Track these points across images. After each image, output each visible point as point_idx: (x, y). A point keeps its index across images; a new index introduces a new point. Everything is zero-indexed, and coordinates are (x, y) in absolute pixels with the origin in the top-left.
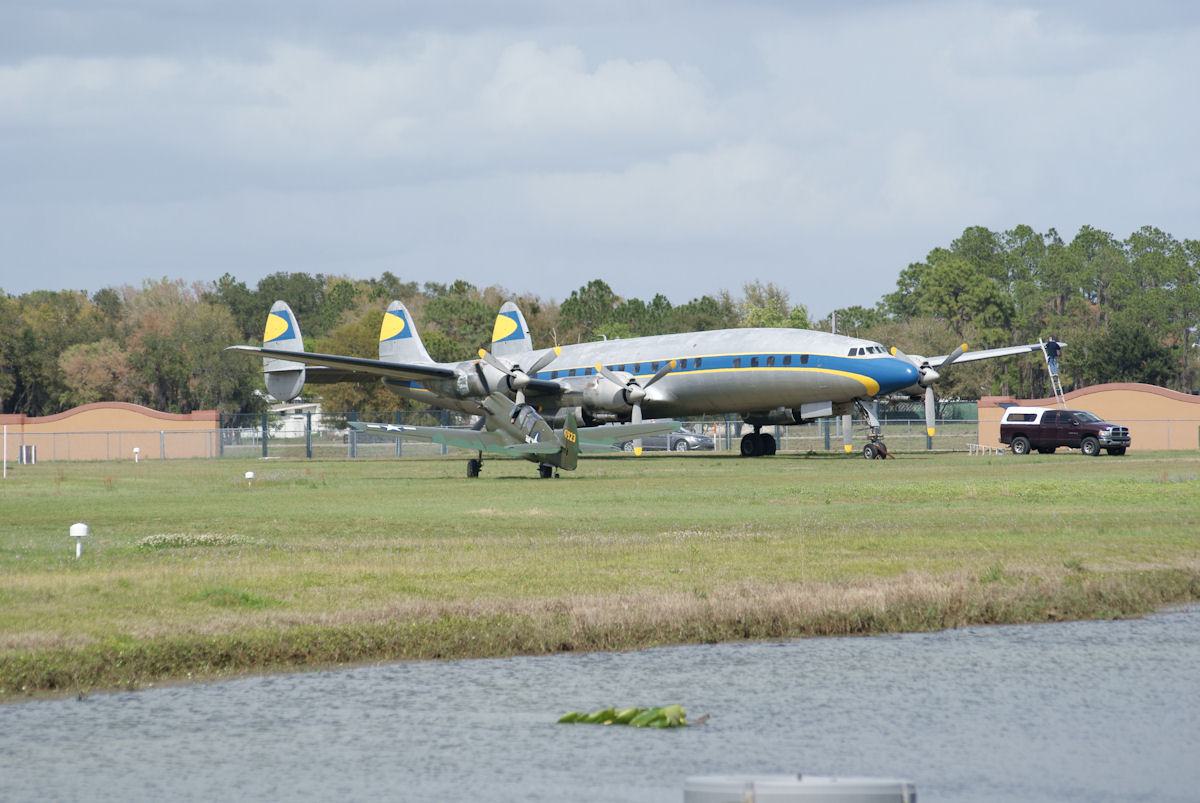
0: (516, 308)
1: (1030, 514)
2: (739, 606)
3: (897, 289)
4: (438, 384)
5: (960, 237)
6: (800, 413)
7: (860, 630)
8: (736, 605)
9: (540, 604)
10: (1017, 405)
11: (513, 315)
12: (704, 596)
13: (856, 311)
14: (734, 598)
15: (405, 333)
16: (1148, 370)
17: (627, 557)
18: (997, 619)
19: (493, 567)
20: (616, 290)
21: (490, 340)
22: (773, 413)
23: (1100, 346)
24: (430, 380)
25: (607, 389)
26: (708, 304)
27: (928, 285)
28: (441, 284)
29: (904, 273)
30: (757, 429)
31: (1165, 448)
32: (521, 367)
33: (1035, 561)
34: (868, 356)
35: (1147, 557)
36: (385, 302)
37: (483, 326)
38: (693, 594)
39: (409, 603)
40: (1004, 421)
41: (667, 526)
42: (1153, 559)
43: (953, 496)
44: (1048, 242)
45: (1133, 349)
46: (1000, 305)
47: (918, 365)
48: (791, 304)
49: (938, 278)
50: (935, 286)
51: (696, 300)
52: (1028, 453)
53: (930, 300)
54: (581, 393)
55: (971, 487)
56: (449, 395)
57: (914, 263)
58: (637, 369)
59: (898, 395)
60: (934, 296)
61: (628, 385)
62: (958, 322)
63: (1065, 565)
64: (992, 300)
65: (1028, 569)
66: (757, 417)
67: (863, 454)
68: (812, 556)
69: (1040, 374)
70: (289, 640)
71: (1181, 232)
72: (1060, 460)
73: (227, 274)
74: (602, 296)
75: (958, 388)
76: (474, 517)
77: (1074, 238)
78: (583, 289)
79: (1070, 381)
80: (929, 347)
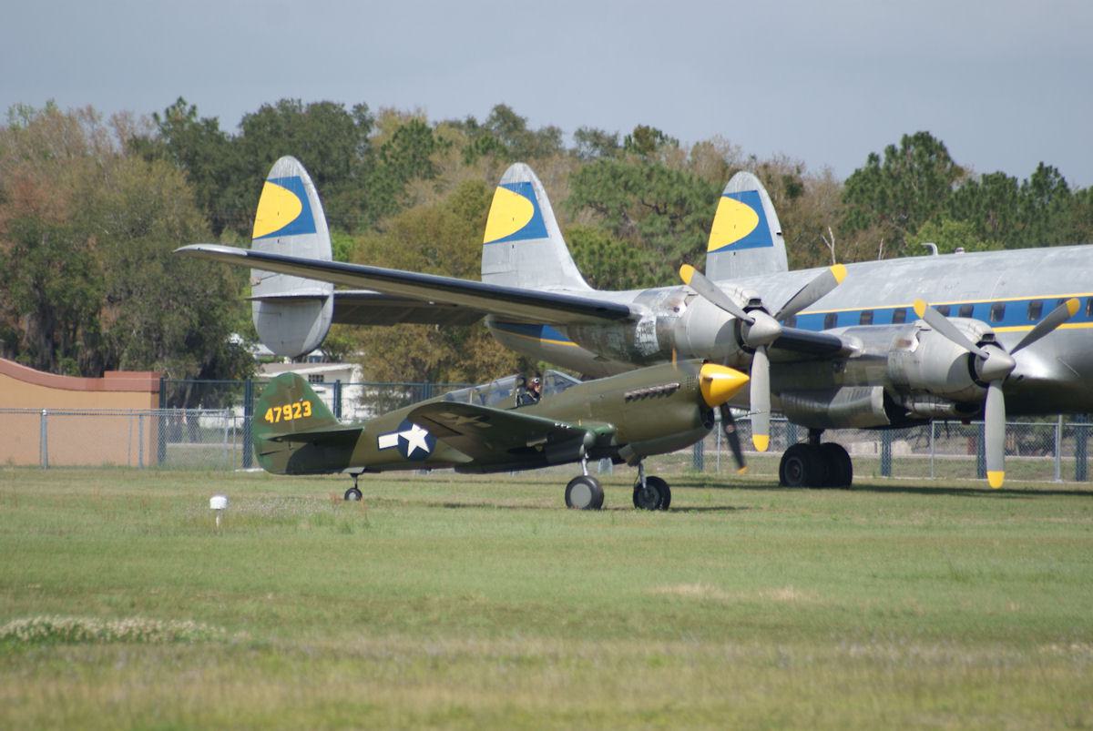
4: (596, 333)
24: (582, 324)
56: (619, 355)
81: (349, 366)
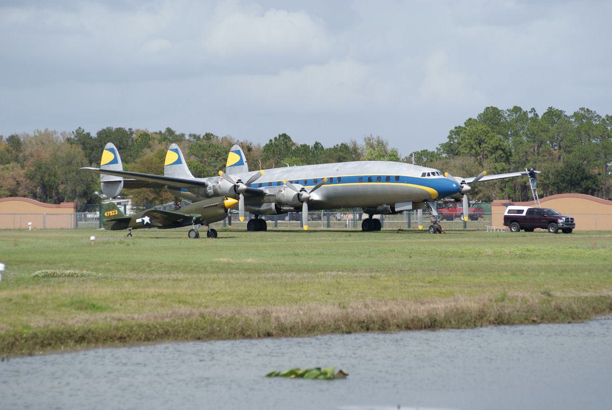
0: (239, 148)
1: (521, 265)
2: (363, 314)
3: (448, 140)
4: (196, 190)
5: (482, 112)
6: (394, 208)
7: (429, 327)
8: (362, 313)
9: (255, 310)
10: (512, 205)
11: (238, 152)
12: (344, 308)
13: (425, 153)
14: (361, 309)
15: (179, 162)
16: (584, 187)
17: (301, 286)
18: (505, 322)
19: (228, 290)
20: (294, 140)
21: (225, 166)
22: (380, 208)
23: (558, 174)
24: (192, 187)
25: (289, 193)
26: (344, 147)
27: (465, 138)
28: (198, 134)
29: (452, 132)
30: (371, 216)
31: (594, 229)
32: (242, 181)
33: (525, 290)
34: (432, 177)
35: (587, 289)
36: (167, 144)
37: (220, 158)
38: (338, 306)
39: (183, 309)
40: (506, 214)
41: (324, 269)
42: (590, 290)
43: (479, 254)
44: (530, 115)
45: (576, 175)
46: (503, 150)
47: (459, 182)
48: (389, 148)
49: (470, 134)
50: (468, 139)
51: (337, 145)
52: (519, 231)
53: (466, 147)
54: (274, 196)
55: (488, 250)
56: (203, 196)
57: (457, 126)
58: (306, 182)
59: (449, 196)
60: (468, 144)
61: (301, 191)
62: (481, 159)
63: (541, 293)
64: (499, 147)
65: (521, 295)
66: (371, 210)
67: (429, 231)
68: (403, 286)
69: (525, 188)
70: (117, 329)
71: (603, 111)
72: (537, 236)
73: (80, 128)
74: (286, 142)
75: (481, 195)
76: (216, 263)
77: (543, 114)
78: (276, 138)
79: (542, 192)
80: (465, 172)
81: (127, 200)
